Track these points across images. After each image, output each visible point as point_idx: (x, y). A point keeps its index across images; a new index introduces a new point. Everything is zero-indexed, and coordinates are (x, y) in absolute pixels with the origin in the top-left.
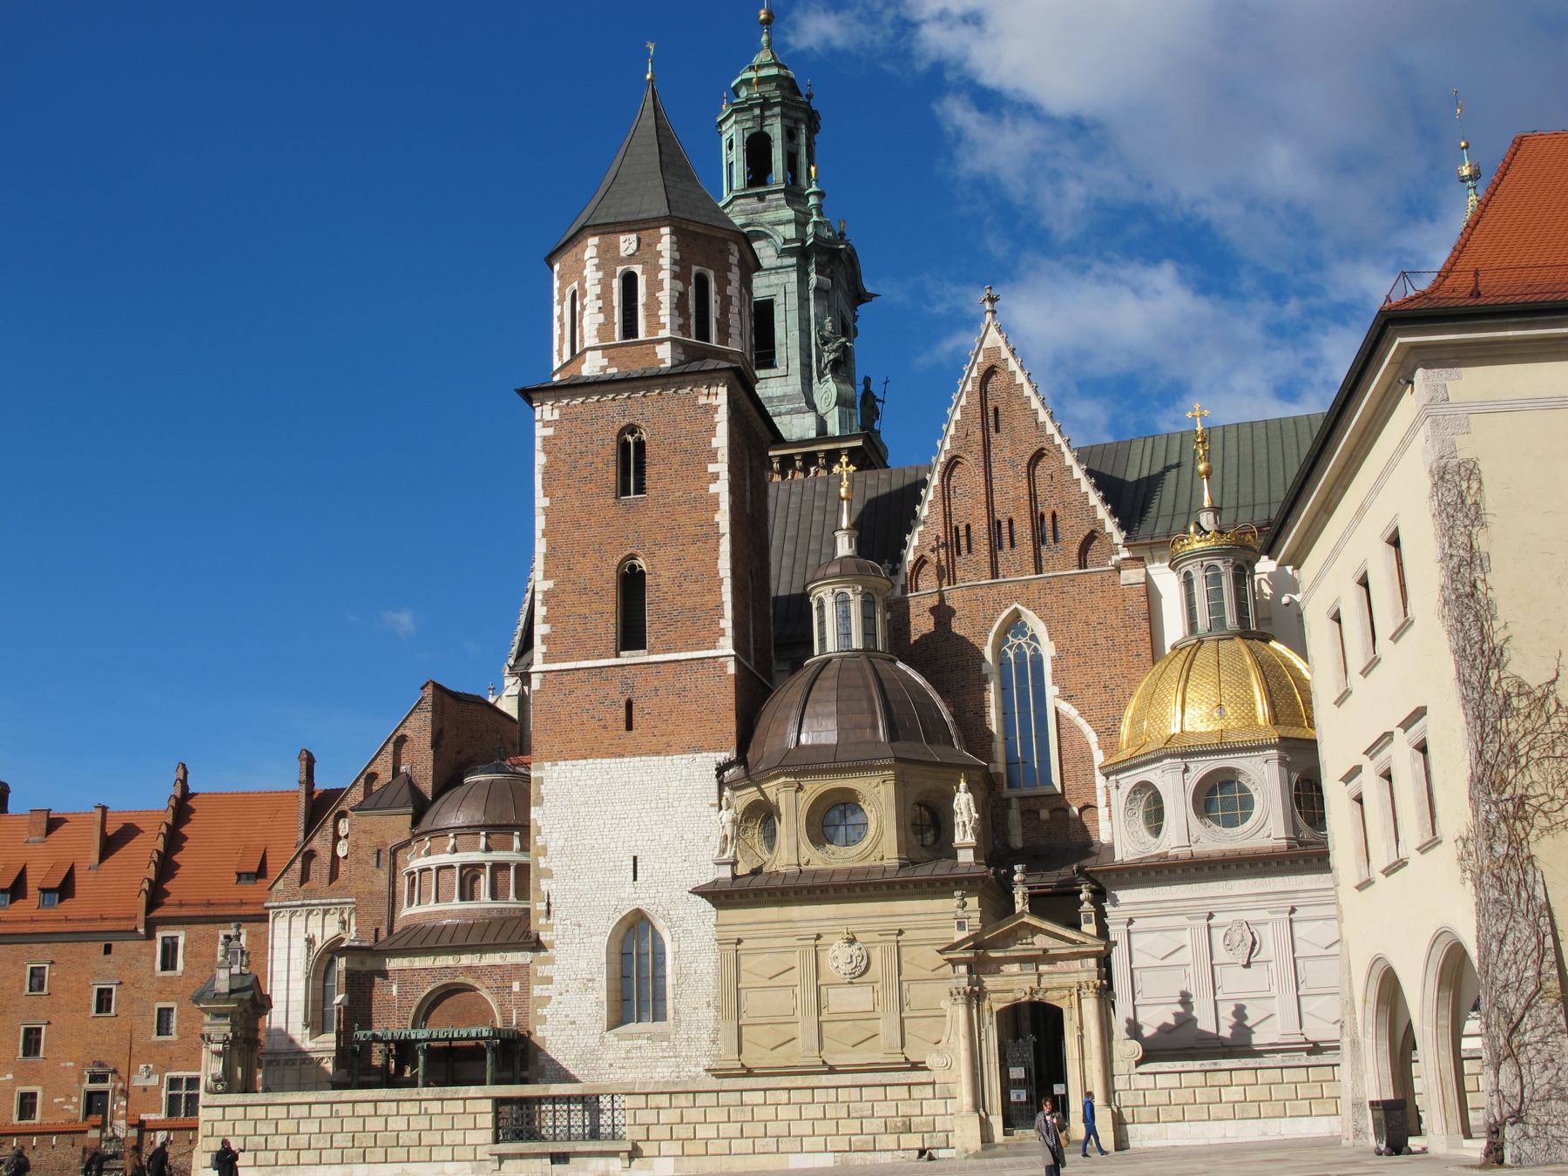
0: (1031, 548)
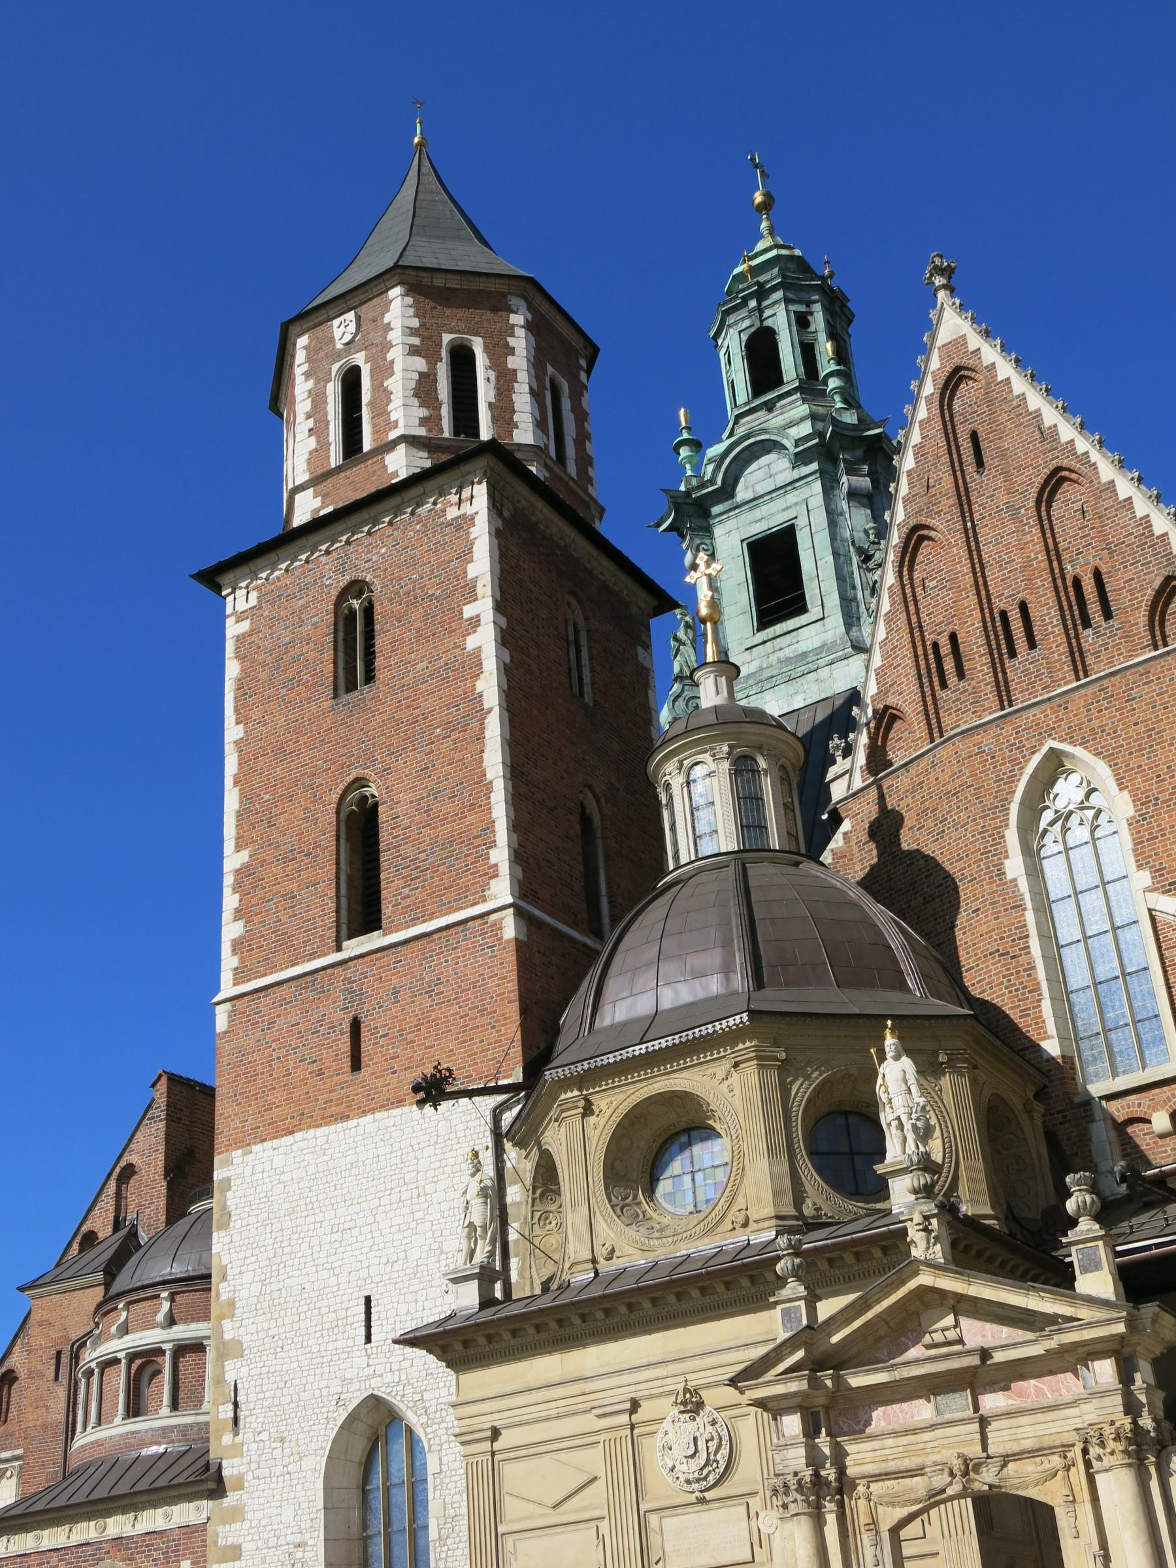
0: (1062, 639)
